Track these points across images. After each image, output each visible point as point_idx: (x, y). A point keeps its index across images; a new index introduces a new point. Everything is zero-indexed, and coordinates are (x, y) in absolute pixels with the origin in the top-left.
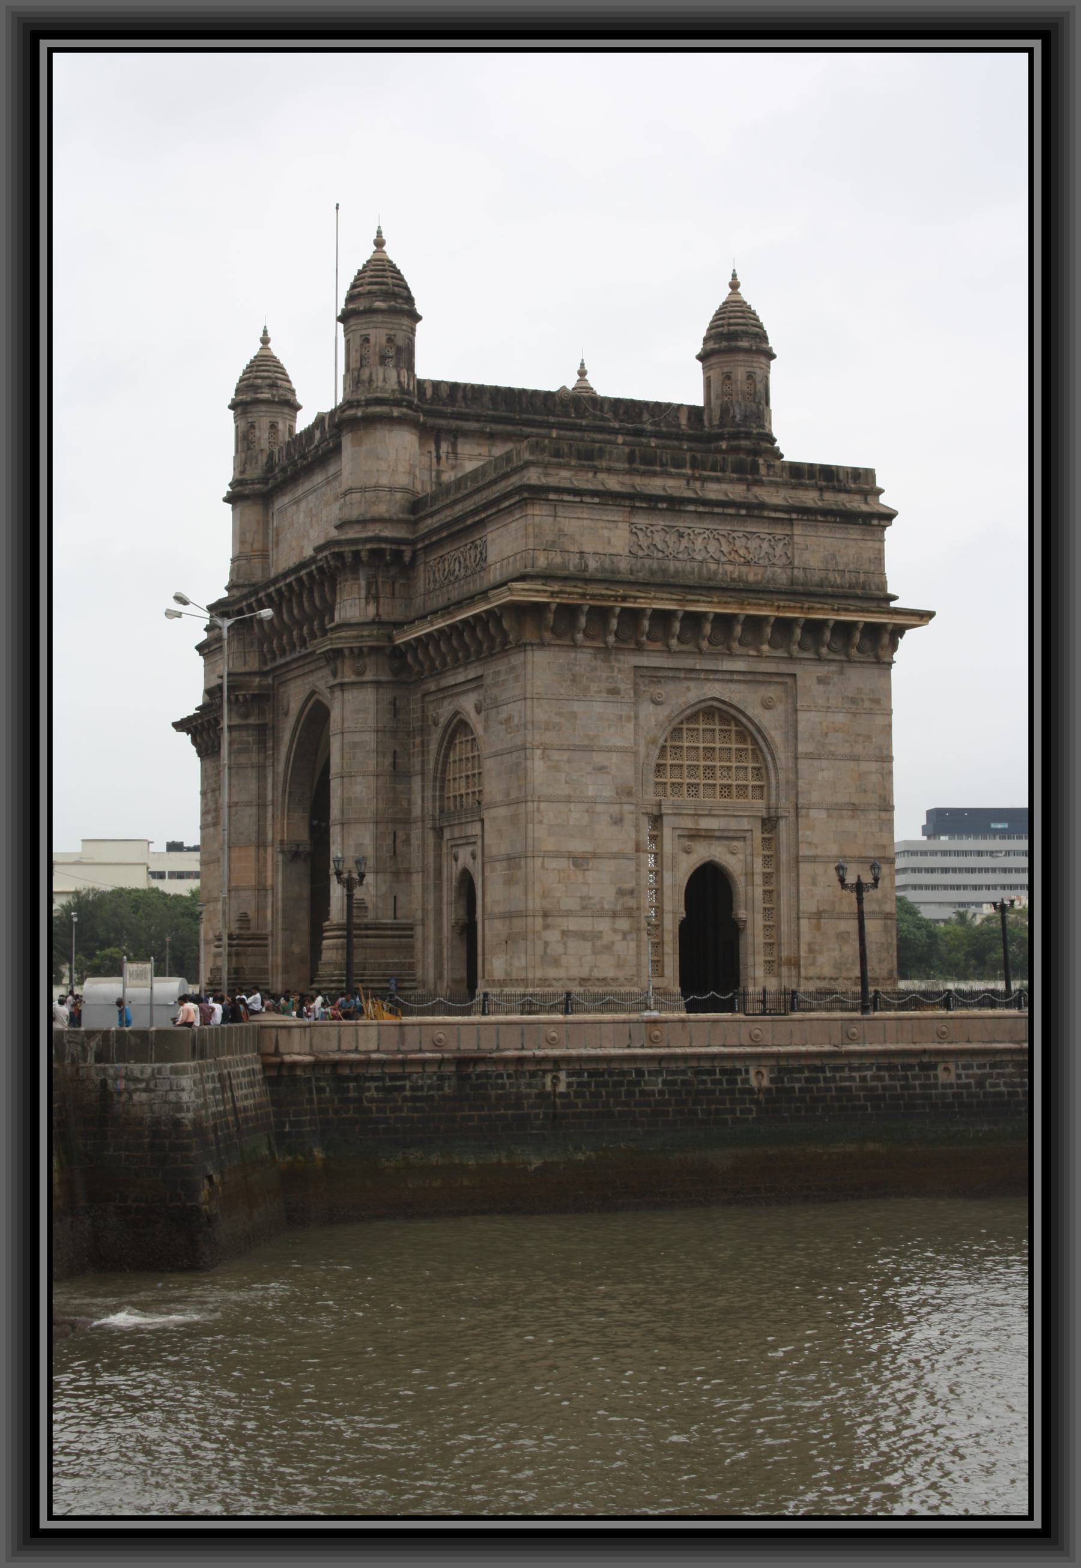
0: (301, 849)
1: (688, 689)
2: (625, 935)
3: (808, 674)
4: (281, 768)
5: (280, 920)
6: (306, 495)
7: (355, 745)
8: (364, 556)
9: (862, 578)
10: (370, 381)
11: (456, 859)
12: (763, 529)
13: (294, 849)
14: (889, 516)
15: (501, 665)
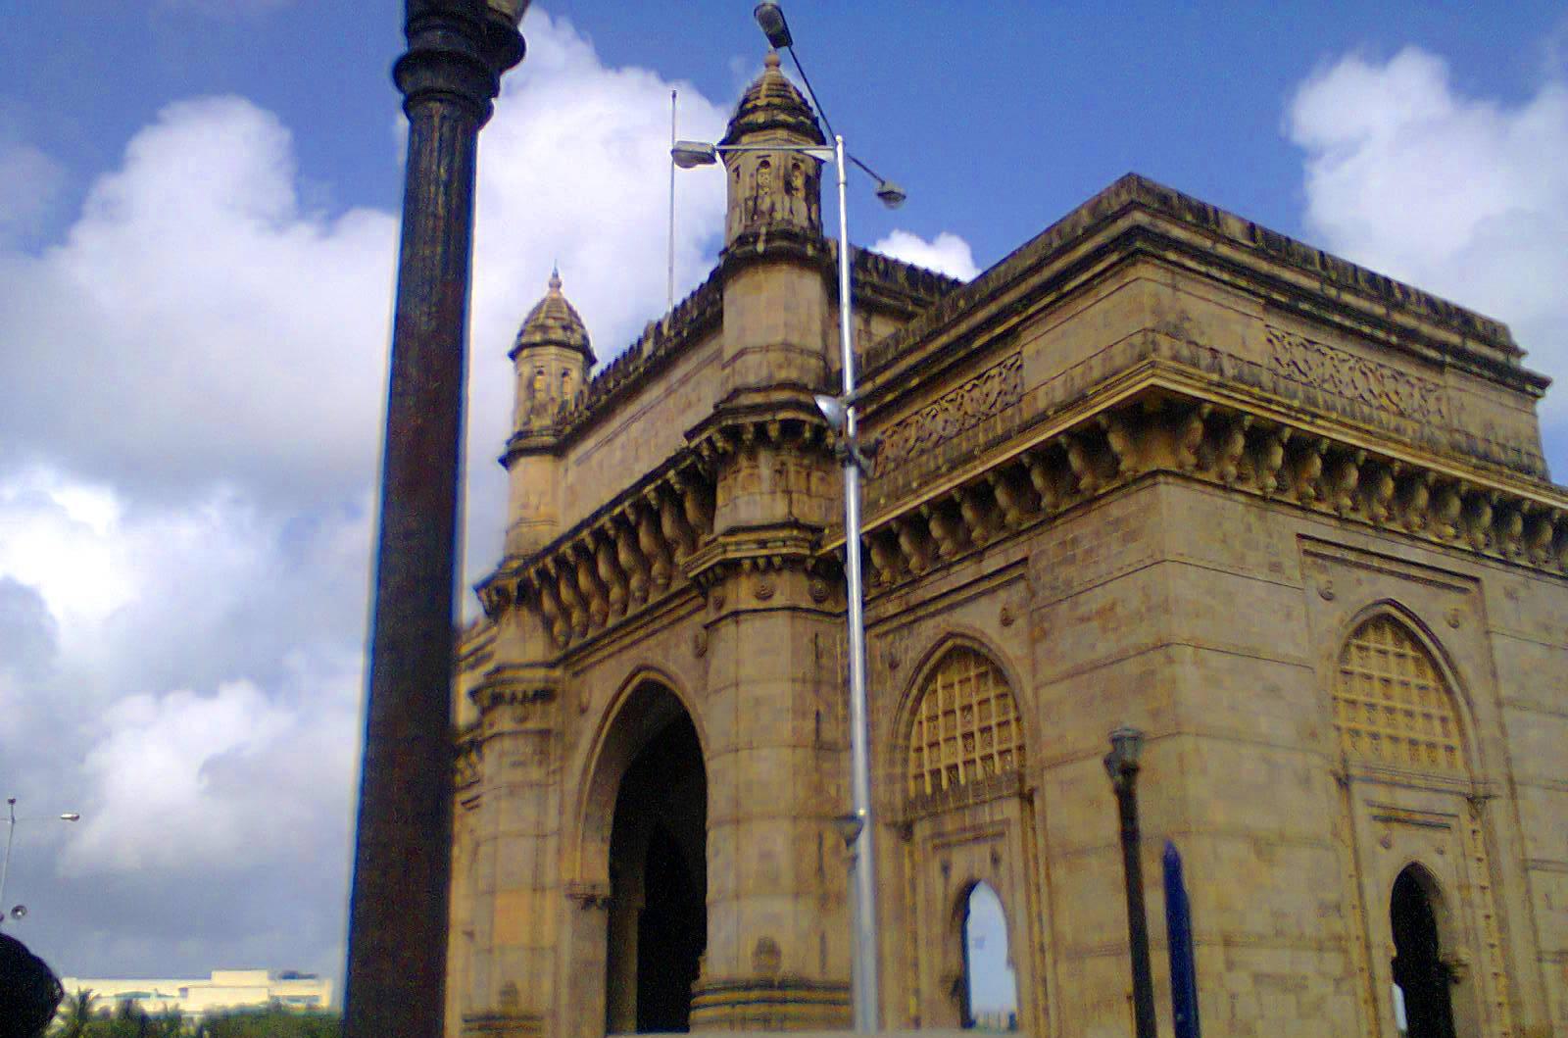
0: (598, 892)
1: (1359, 582)
2: (1338, 982)
3: (1496, 579)
4: (572, 782)
5: (564, 992)
6: (625, 427)
7: (758, 702)
8: (774, 431)
9: (1526, 460)
10: (772, 209)
11: (946, 869)
12: (1412, 371)
13: (589, 892)
14: (1543, 383)
15: (1085, 529)
